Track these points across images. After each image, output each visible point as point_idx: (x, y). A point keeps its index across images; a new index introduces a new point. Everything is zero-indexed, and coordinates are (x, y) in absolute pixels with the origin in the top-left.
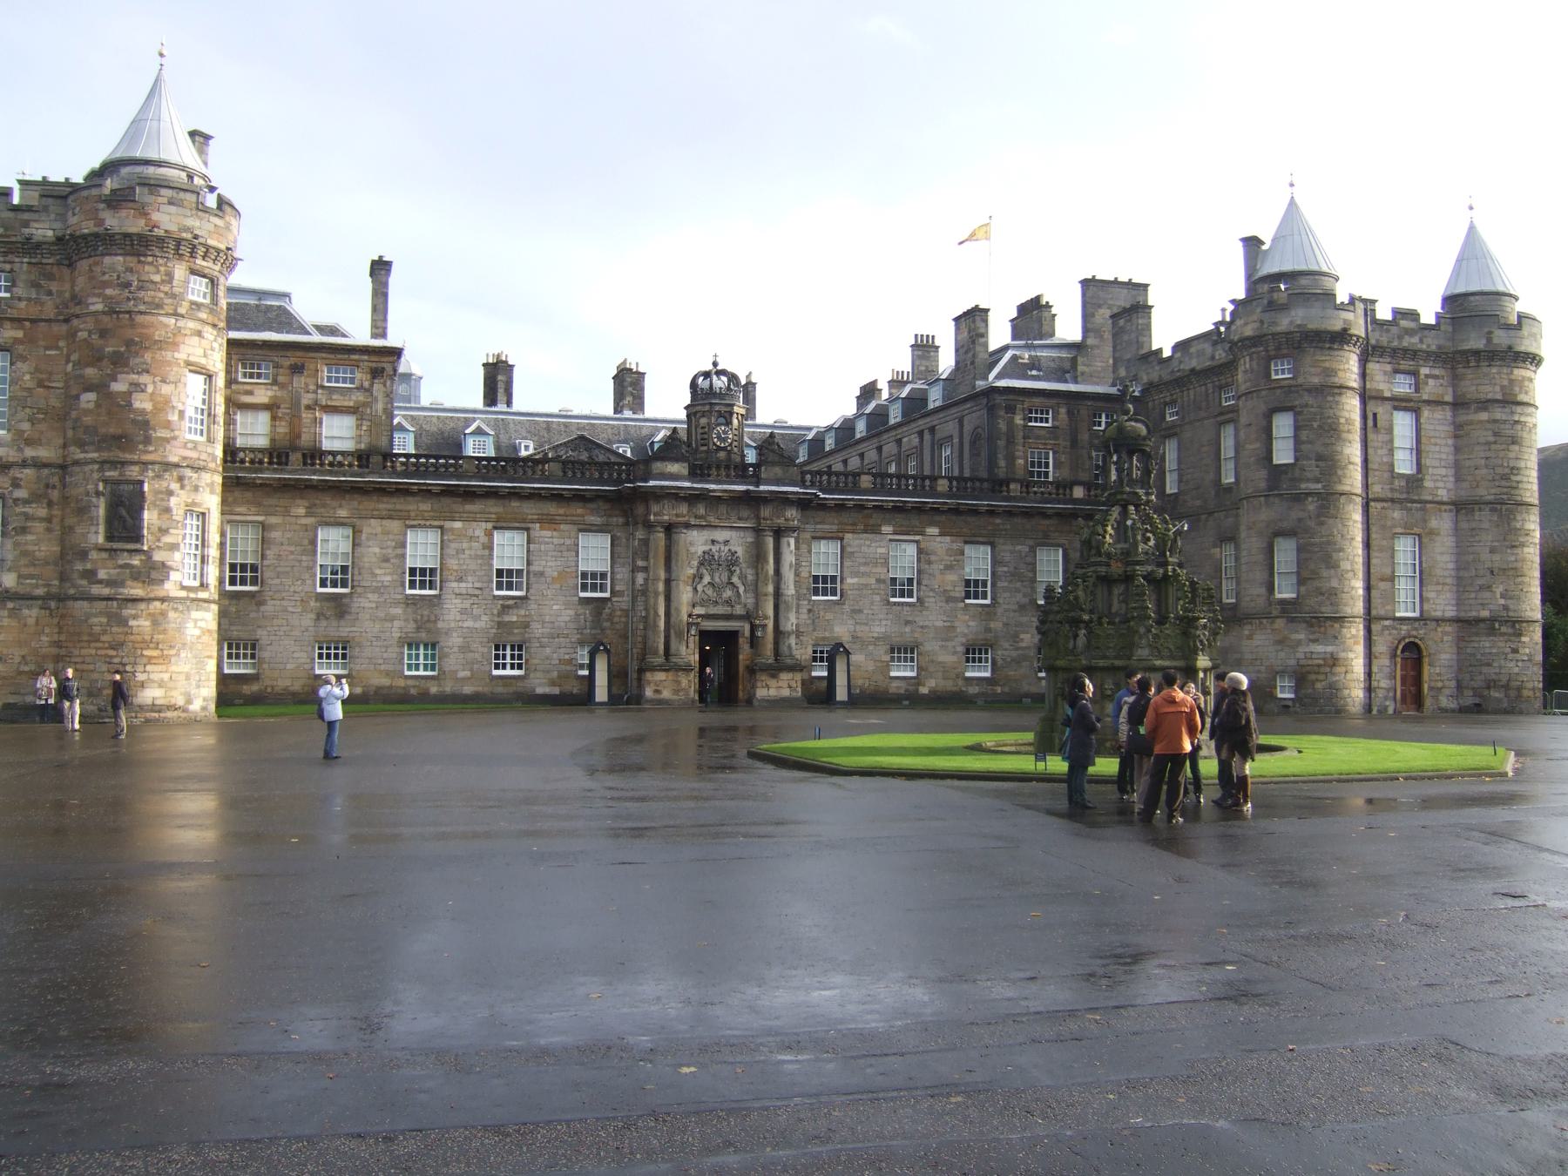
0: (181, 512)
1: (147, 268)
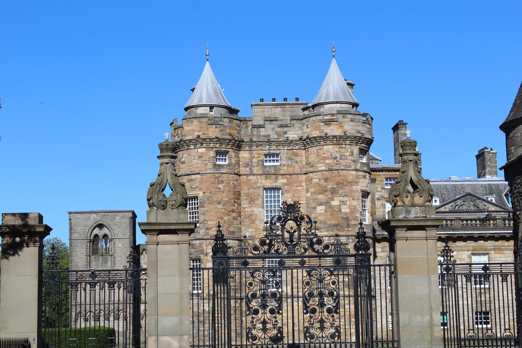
1: (343, 149)
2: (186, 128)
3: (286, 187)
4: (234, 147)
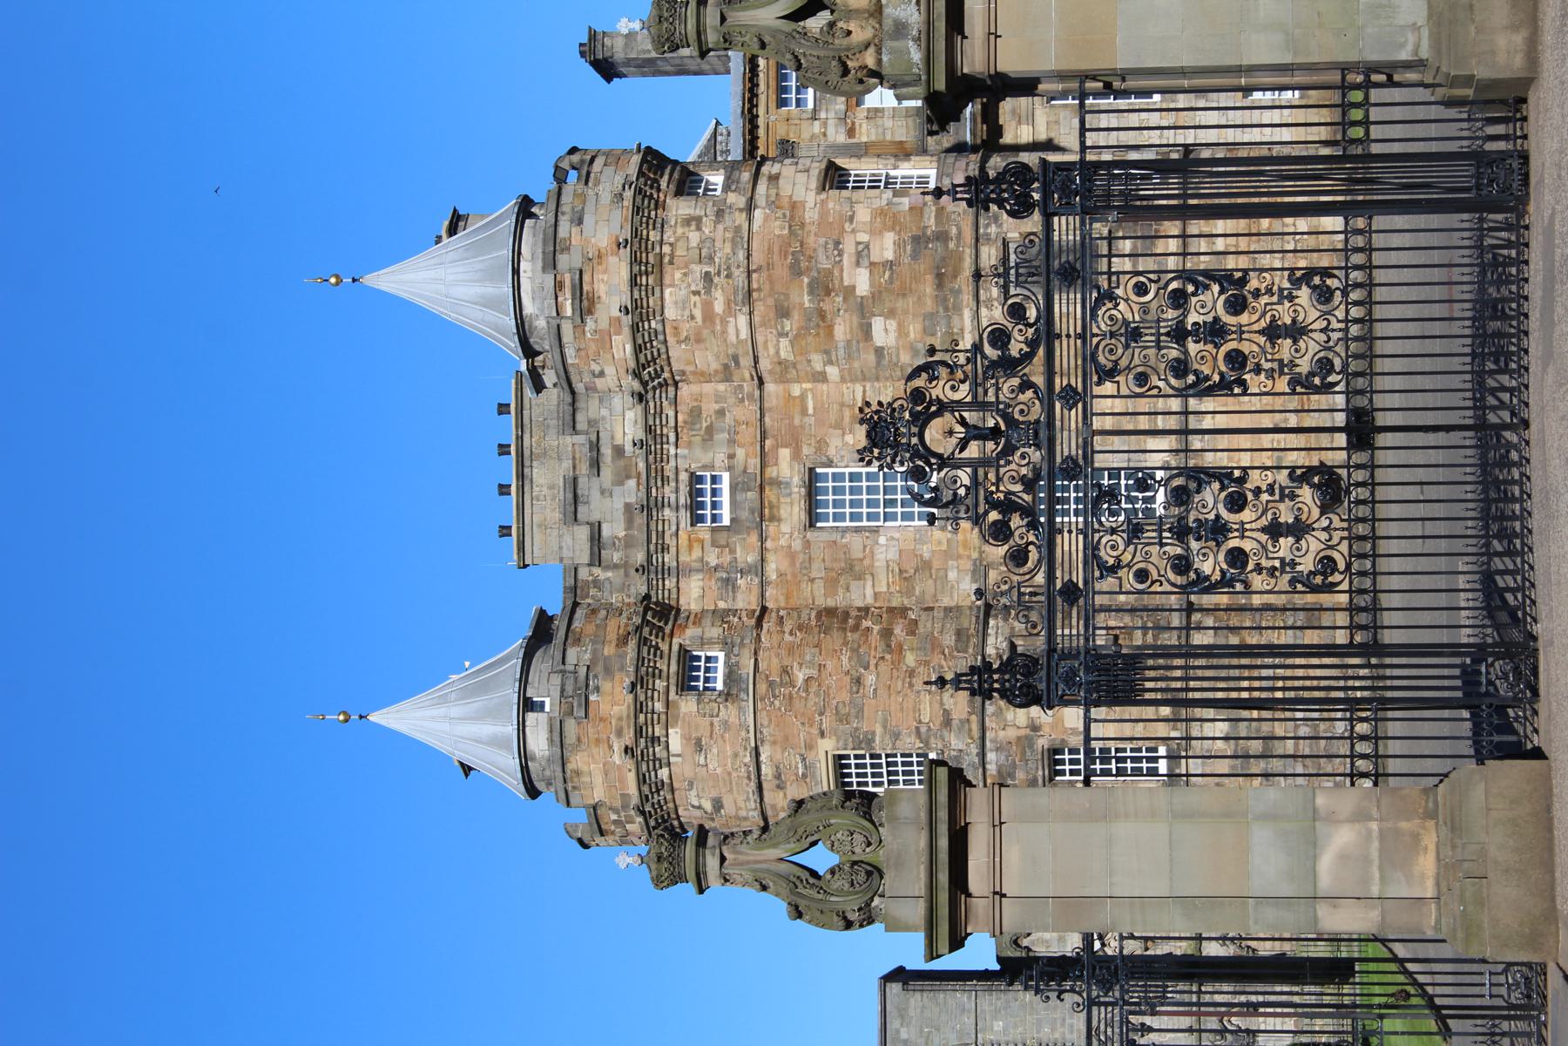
1: (679, 252)
2: (598, 794)
3: (806, 450)
4: (668, 629)
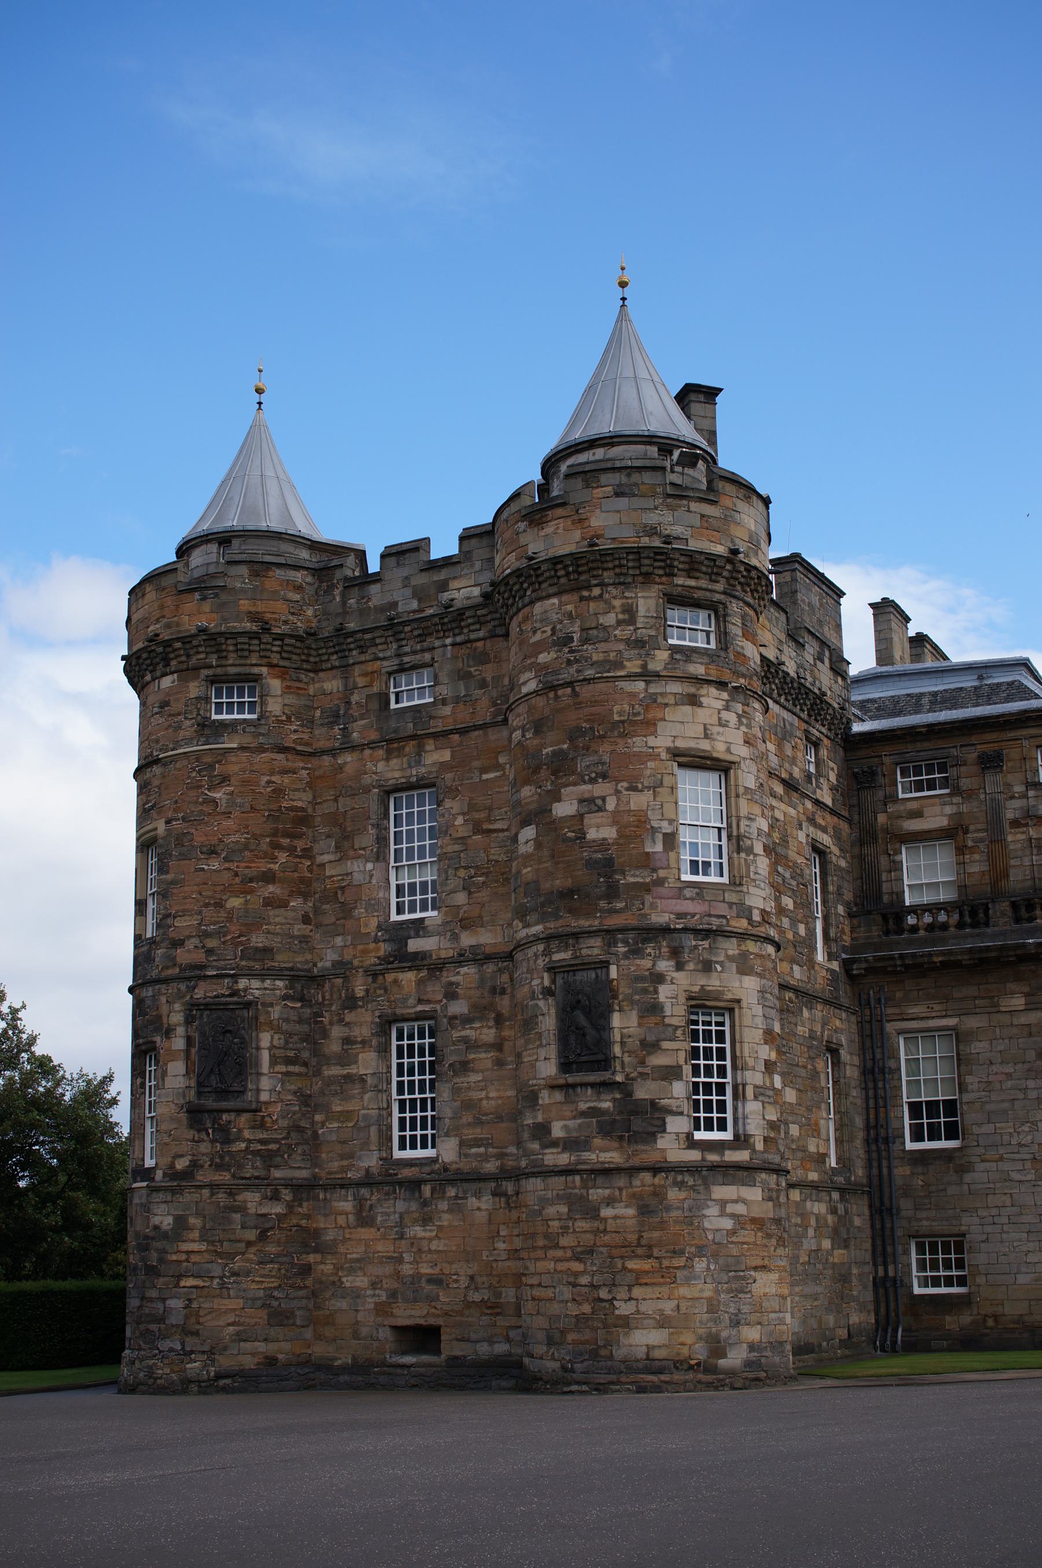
0: (681, 1010)
3: (449, 776)
